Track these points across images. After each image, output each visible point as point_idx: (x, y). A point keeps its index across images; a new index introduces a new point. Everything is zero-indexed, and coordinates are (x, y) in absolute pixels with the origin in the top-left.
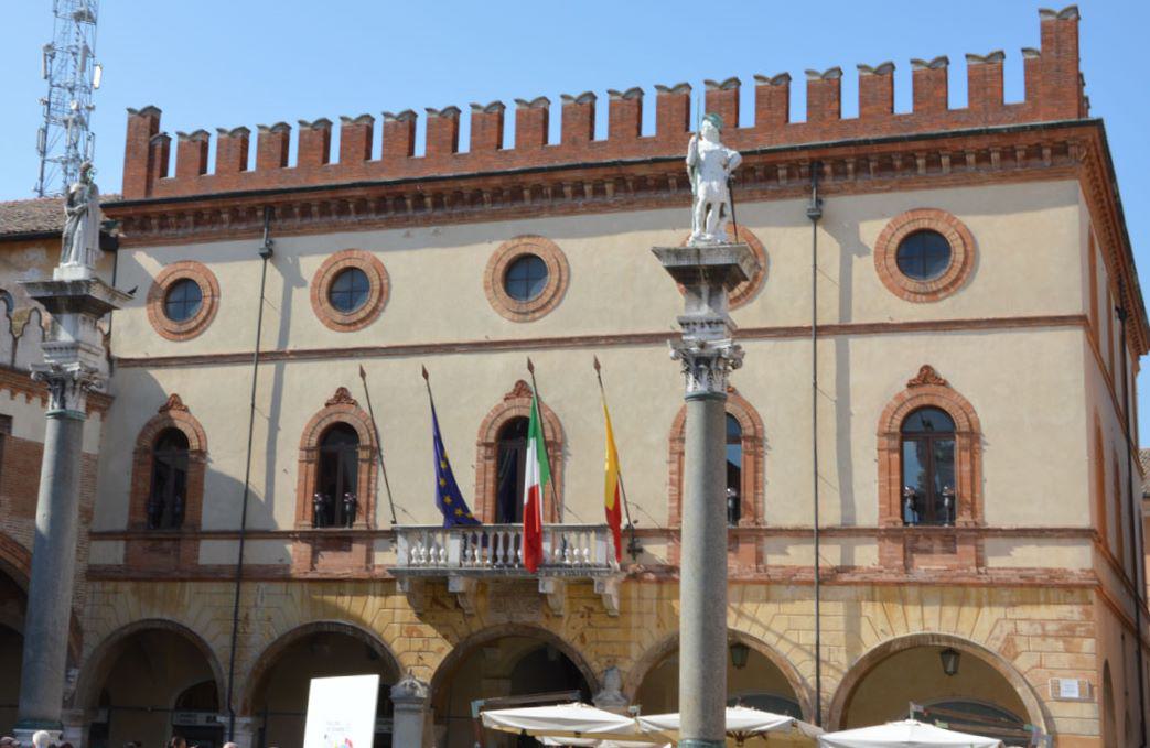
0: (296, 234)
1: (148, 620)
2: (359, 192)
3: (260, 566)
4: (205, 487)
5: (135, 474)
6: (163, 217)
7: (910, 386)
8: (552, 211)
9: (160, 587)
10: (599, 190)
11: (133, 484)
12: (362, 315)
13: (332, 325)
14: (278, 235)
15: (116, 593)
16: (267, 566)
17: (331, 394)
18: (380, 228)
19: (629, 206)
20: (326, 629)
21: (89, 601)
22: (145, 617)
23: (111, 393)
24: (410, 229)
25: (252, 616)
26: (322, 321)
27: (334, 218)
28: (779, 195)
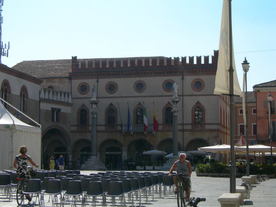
2: (113, 72)
7: (196, 104)
8: (143, 76)
10: (151, 73)
13: (109, 93)
19: (155, 76)
24: (121, 78)
28: (178, 75)
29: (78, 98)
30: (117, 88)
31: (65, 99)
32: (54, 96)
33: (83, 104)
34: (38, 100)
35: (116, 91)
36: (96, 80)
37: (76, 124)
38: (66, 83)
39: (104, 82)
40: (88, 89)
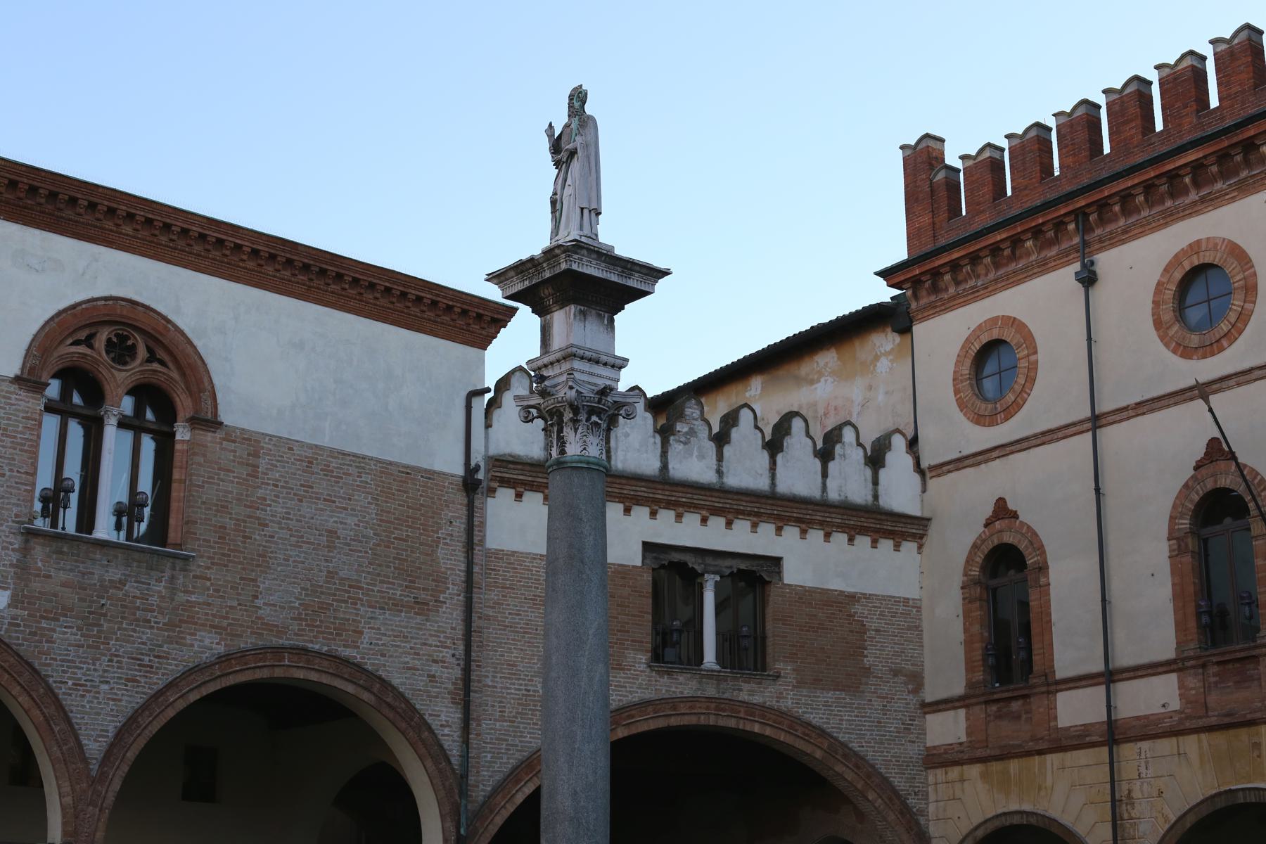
0: (1123, 242)
1: (1004, 814)
2: (1192, 156)
3: (1138, 718)
4: (1054, 617)
5: (967, 615)
6: (955, 266)
9: (1014, 765)
11: (966, 630)
12: (1225, 327)
13: (1186, 352)
14: (1100, 250)
15: (962, 780)
16: (1146, 717)
17: (1200, 451)
18: (1233, 200)
20: (1241, 799)
21: (932, 797)
22: (1000, 811)
23: (926, 515)
25: (1136, 794)
26: (1174, 352)
27: (1169, 203)
29: (959, 463)
30: (1250, 289)
31: (825, 475)
32: (676, 448)
33: (1001, 505)
34: (459, 470)
35: (1244, 318)
36: (1077, 266)
37: (959, 689)
38: (883, 365)
39: (1139, 263)
40: (1023, 364)
